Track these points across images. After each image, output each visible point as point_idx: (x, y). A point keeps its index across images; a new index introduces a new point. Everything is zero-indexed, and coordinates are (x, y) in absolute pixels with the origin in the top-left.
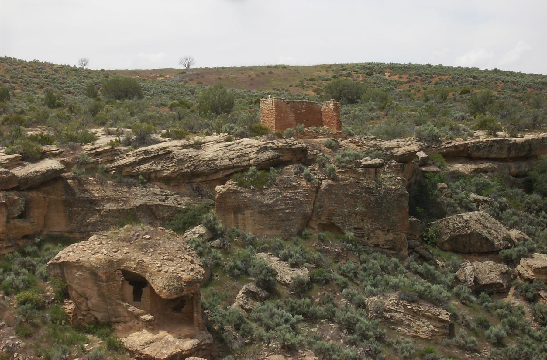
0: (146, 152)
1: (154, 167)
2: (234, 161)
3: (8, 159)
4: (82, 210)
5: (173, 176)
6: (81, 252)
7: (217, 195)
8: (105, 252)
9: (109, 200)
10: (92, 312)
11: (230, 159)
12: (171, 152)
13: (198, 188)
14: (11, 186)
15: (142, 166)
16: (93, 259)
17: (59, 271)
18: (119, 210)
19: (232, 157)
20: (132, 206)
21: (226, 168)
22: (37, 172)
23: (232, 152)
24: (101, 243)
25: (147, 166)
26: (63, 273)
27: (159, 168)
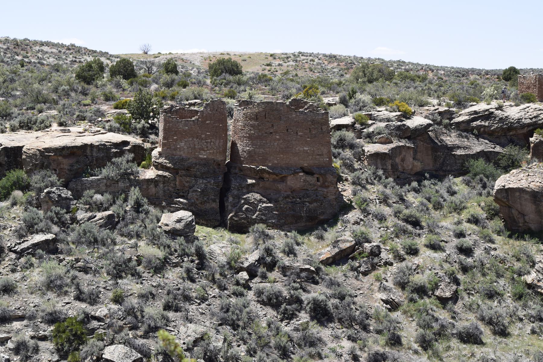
0: (475, 112)
1: (483, 123)
2: (534, 120)
3: (396, 116)
4: (443, 154)
5: (497, 130)
6: (518, 182)
7: (532, 145)
8: (540, 181)
9: (459, 147)
10: (526, 224)
11: (531, 119)
12: (493, 112)
13: (511, 139)
14: (406, 136)
15: (475, 123)
16: (532, 186)
17: (505, 194)
18: (467, 155)
19: (531, 117)
20: (474, 152)
21: (529, 125)
22: (421, 125)
23: (529, 114)
24: (529, 175)
25: (478, 123)
26: (508, 195)
27: (487, 124)
